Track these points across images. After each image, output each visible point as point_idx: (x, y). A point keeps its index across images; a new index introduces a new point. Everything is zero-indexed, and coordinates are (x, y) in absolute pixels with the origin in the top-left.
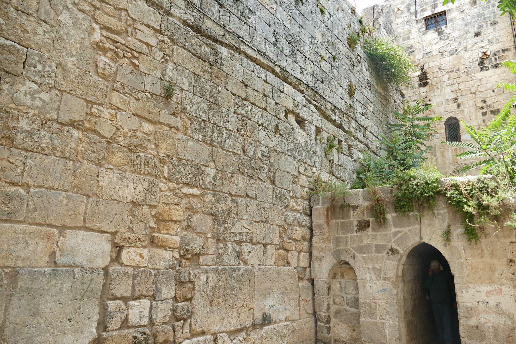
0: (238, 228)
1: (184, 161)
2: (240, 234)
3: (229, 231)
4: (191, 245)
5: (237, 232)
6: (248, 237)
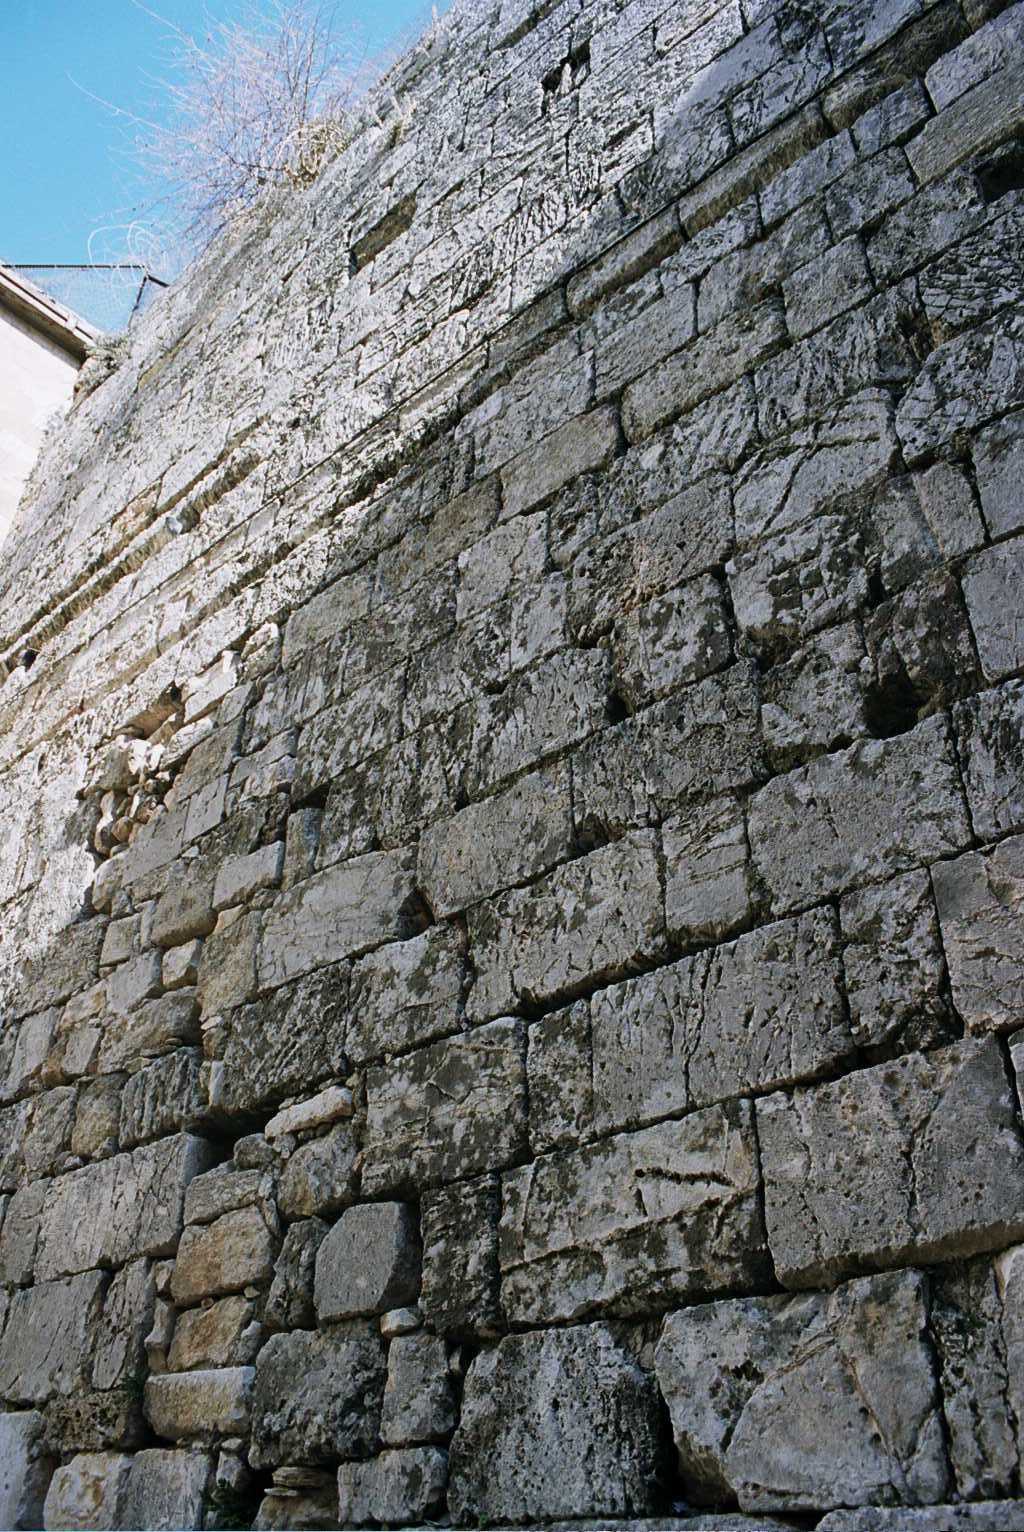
0: (608, 1198)
1: (281, 993)
2: (629, 1241)
3: (531, 1252)
4: (291, 1403)
5: (599, 1233)
6: (713, 1245)
